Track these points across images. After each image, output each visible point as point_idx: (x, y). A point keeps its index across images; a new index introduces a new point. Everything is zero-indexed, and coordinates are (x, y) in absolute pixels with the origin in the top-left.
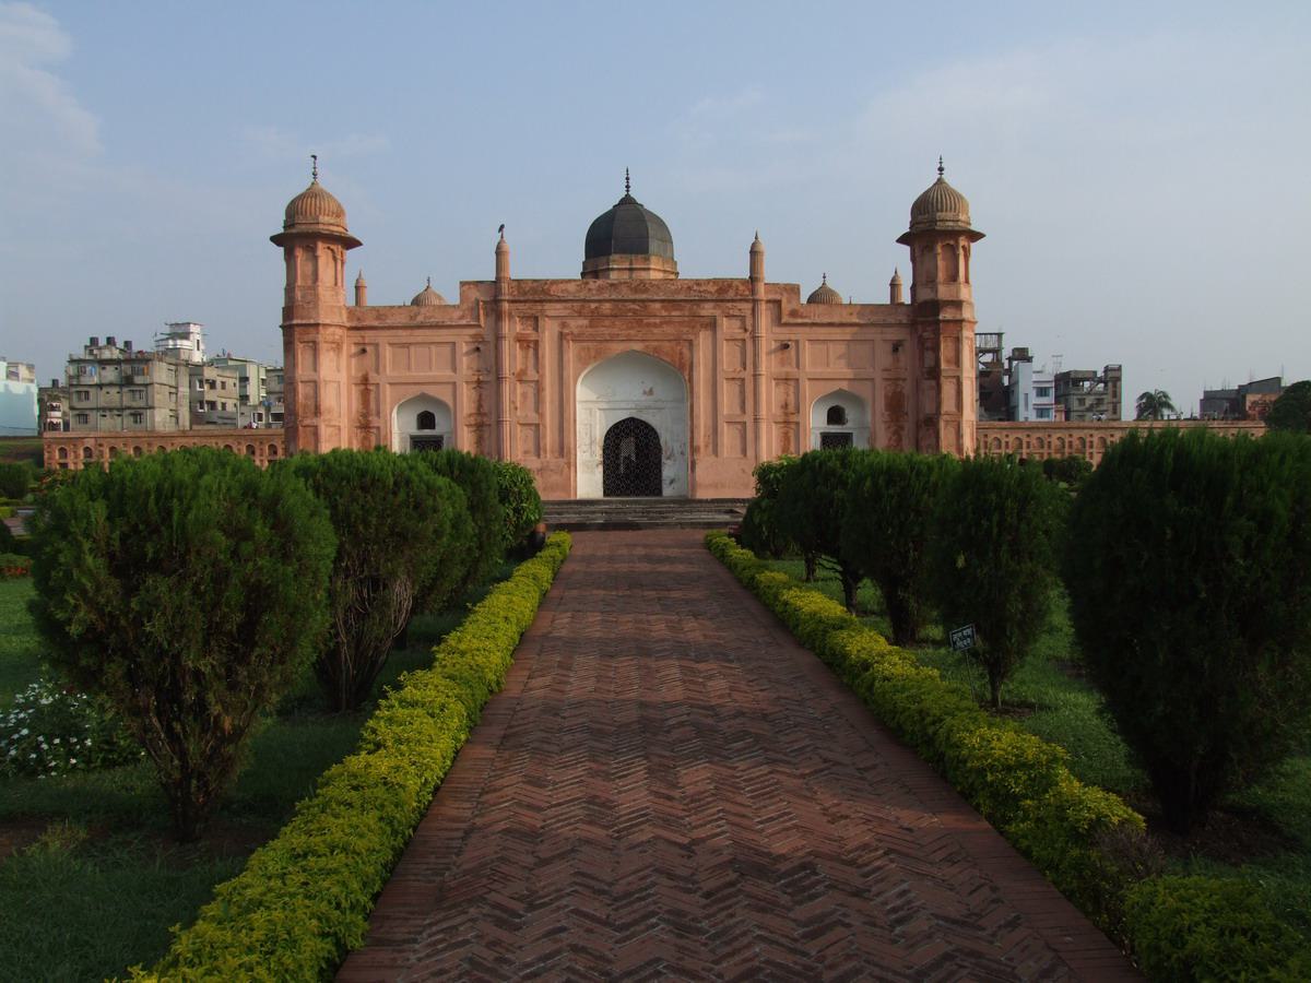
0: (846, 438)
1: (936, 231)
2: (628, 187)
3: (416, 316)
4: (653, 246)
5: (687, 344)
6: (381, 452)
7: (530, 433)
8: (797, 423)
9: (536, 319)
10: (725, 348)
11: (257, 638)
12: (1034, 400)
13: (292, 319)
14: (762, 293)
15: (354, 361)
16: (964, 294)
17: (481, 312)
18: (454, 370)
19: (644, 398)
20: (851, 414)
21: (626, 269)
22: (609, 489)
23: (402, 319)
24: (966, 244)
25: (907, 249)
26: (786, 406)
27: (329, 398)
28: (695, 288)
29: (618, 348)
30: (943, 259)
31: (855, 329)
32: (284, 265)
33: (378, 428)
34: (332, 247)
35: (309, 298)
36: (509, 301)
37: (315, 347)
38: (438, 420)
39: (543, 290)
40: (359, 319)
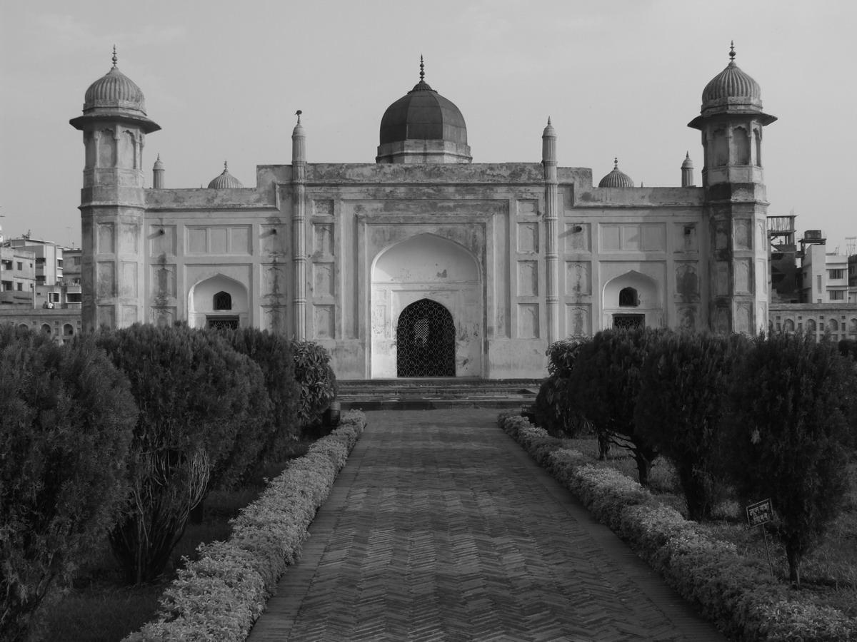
0: (638, 319)
1: (727, 115)
2: (422, 74)
3: (213, 198)
4: (447, 131)
5: (480, 227)
6: (181, 327)
7: (325, 314)
8: (590, 305)
9: (332, 202)
12: (828, 282)
13: (91, 201)
14: (554, 177)
15: (151, 242)
16: (756, 176)
17: (278, 195)
18: (251, 251)
19: (438, 280)
20: (642, 295)
21: (420, 154)
23: (200, 202)
24: (758, 127)
25: (697, 134)
26: (578, 288)
27: (126, 279)
28: (488, 172)
29: (412, 231)
30: (735, 142)
31: (646, 212)
32: (83, 147)
33: (175, 308)
34: (131, 130)
35: (108, 180)
36: (304, 184)
37: (113, 228)
38: (235, 300)
40: (157, 201)
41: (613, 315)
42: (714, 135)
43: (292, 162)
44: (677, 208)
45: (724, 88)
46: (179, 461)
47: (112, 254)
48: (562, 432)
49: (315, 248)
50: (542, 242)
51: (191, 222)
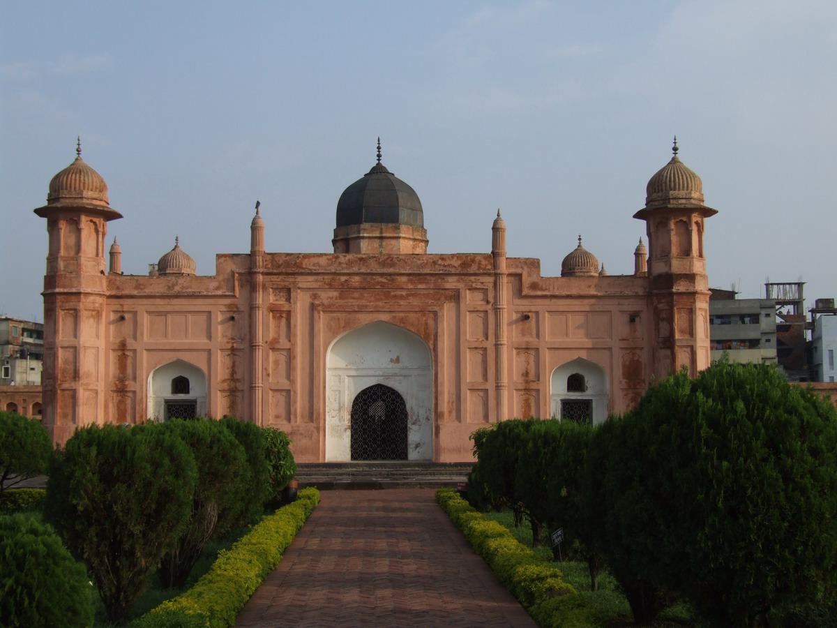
0: (586, 406)
1: (670, 207)
2: (379, 156)
4: (403, 214)
5: (432, 315)
6: (201, 421)
7: (282, 398)
8: (538, 391)
9: (289, 291)
10: (468, 319)
11: (163, 517)
13: (55, 288)
14: (503, 267)
15: (112, 327)
16: (697, 267)
17: (237, 283)
18: (210, 338)
19: (391, 365)
20: (589, 381)
22: (355, 454)
24: (699, 220)
25: (642, 224)
26: (526, 374)
27: (88, 363)
28: (440, 262)
29: (365, 318)
30: (676, 234)
31: (592, 301)
32: (46, 235)
33: (134, 392)
34: (94, 220)
35: (71, 268)
36: (263, 274)
38: (193, 384)
39: (296, 263)
40: (118, 288)
41: (562, 400)
42: (657, 227)
43: (251, 252)
44: (622, 297)
45: (666, 183)
46: (200, 507)
47: (74, 339)
48: (490, 507)
49: (272, 335)
50: (490, 329)
51: (152, 309)
